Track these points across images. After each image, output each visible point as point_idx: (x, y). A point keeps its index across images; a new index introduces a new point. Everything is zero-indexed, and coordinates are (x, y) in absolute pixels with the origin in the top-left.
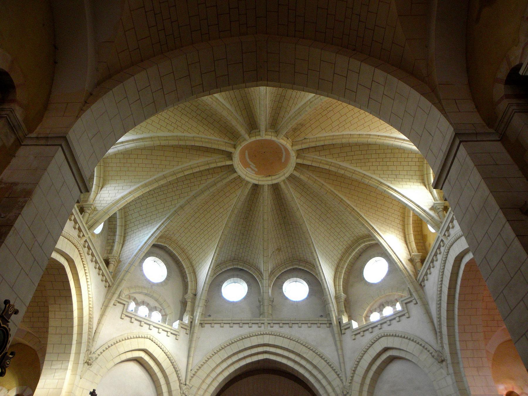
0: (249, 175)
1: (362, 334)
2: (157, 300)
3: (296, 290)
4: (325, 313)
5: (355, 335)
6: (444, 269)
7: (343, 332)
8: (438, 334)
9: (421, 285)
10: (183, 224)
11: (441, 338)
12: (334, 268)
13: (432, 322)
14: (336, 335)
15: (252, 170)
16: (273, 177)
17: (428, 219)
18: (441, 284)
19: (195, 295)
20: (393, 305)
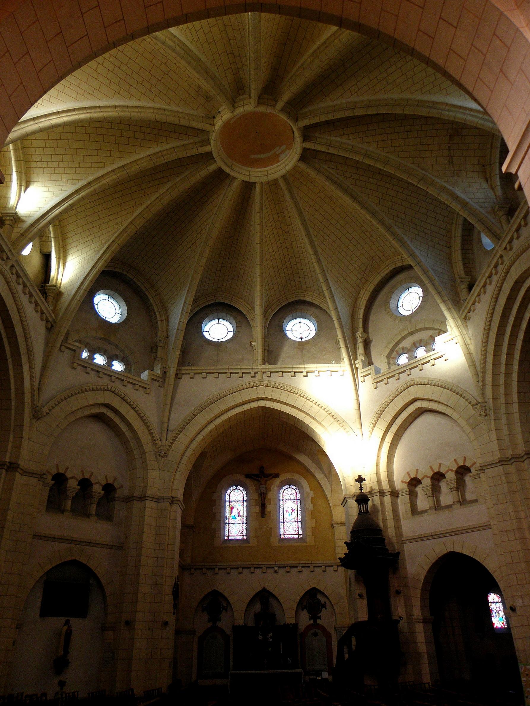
0: (288, 160)
2: (426, 329)
15: (283, 152)
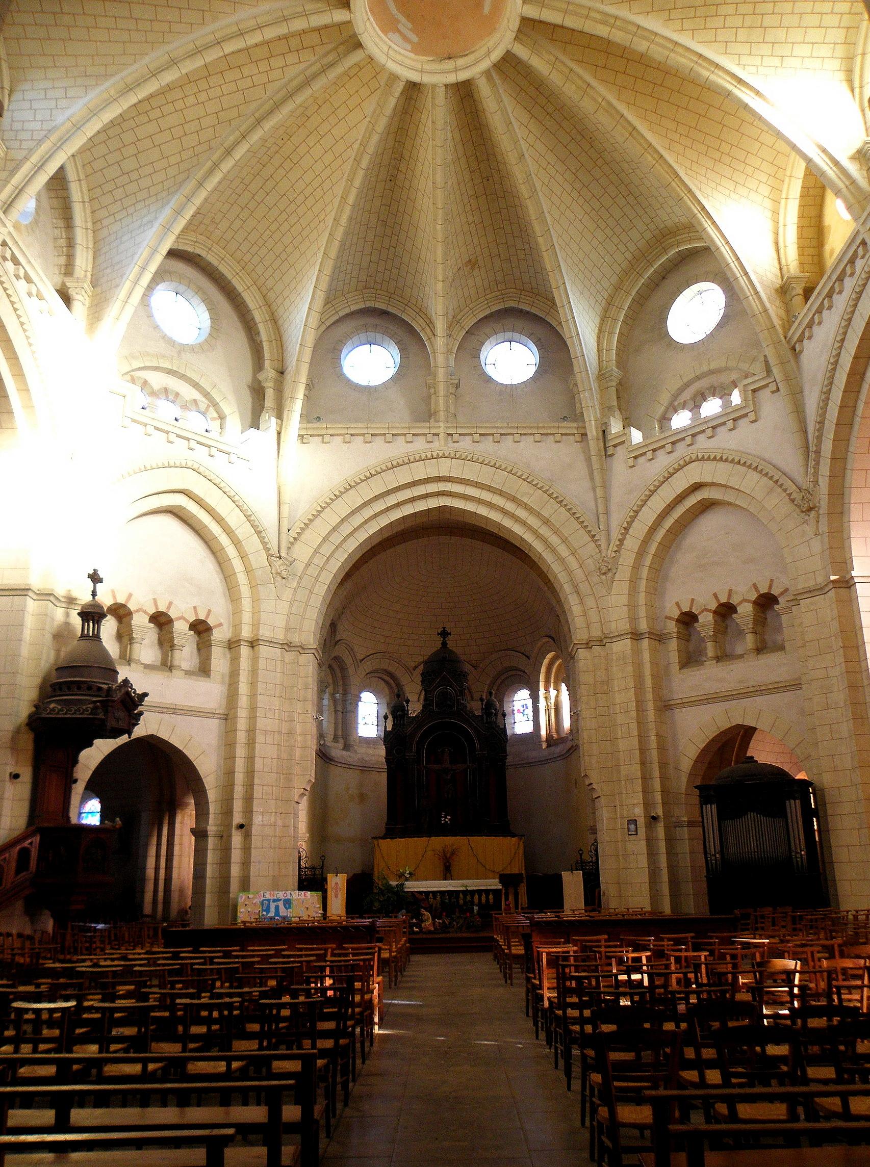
1: (649, 455)
2: (196, 385)
3: (511, 361)
4: (572, 412)
5: (635, 458)
6: (853, 312)
7: (609, 453)
8: (812, 455)
9: (794, 349)
10: (235, 196)
11: (818, 463)
12: (599, 309)
13: (804, 431)
14: (594, 459)
15: (405, 38)
16: (461, 62)
17: (841, 185)
18: (840, 348)
19: (282, 373)
20: (723, 392)
